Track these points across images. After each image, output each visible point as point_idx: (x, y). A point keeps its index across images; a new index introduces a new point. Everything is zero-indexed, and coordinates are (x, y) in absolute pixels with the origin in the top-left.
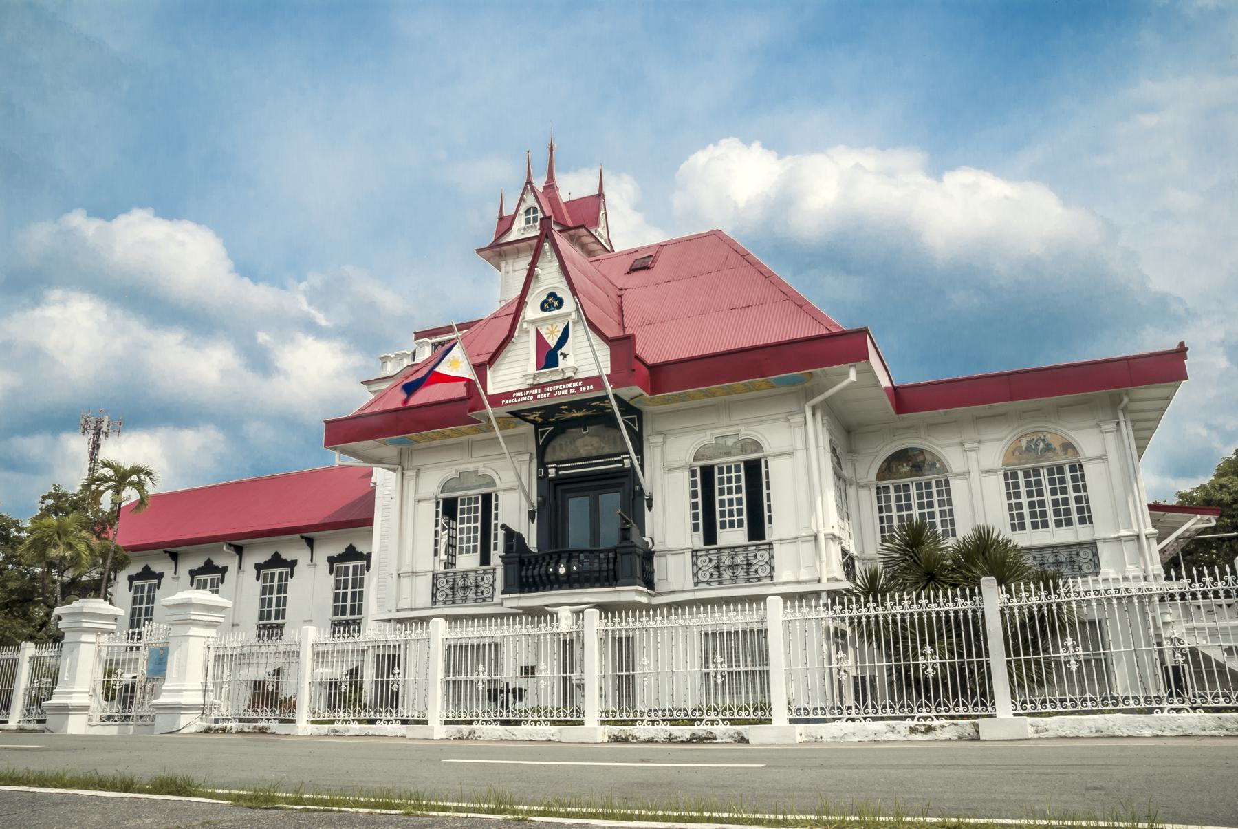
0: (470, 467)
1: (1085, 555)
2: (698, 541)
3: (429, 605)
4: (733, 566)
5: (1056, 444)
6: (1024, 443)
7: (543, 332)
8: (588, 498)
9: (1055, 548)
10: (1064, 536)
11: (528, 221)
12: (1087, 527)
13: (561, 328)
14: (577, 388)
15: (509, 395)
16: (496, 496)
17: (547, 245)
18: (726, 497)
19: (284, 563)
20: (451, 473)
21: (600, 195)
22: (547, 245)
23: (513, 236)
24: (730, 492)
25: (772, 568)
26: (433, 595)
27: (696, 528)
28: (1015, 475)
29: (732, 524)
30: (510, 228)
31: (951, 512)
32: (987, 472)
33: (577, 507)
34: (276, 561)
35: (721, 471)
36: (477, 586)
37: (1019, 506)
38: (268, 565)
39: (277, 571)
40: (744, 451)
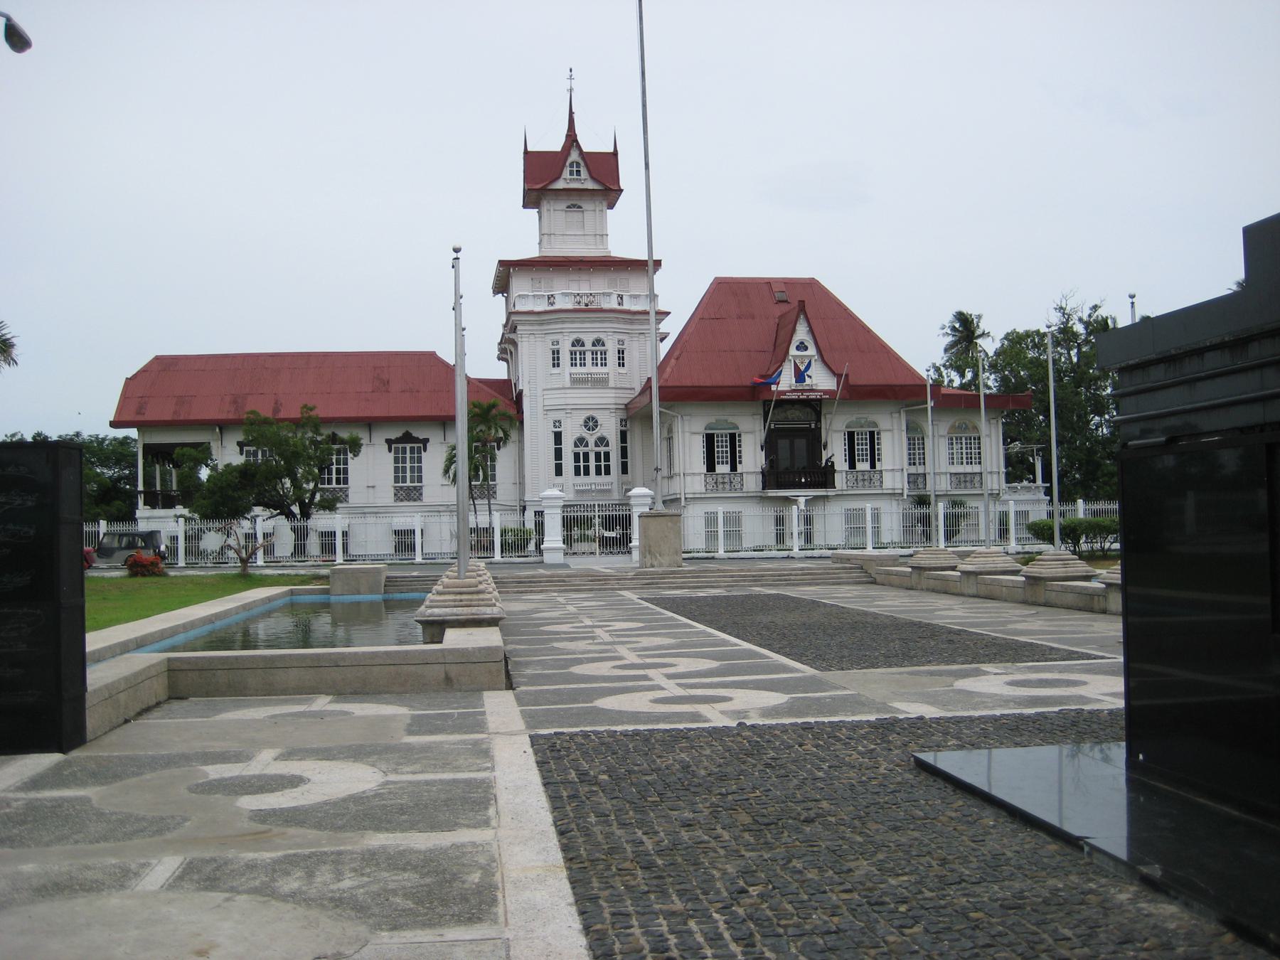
0: (722, 418)
1: (977, 478)
2: (846, 467)
3: (704, 491)
4: (864, 480)
5: (970, 426)
6: (957, 424)
7: (797, 362)
8: (788, 441)
9: (965, 474)
10: (969, 469)
11: (571, 173)
12: (978, 466)
13: (807, 361)
14: (821, 396)
15: (784, 393)
16: (740, 436)
17: (802, 317)
18: (860, 447)
19: (417, 440)
20: (712, 419)
21: (615, 154)
22: (802, 317)
23: (560, 185)
24: (862, 445)
25: (882, 482)
26: (705, 486)
27: (846, 461)
28: (952, 439)
29: (863, 461)
30: (558, 178)
31: (924, 454)
32: (941, 436)
33: (783, 444)
34: (407, 438)
35: (858, 435)
36: (731, 482)
37: (953, 454)
38: (398, 441)
39: (408, 446)
40: (869, 427)
